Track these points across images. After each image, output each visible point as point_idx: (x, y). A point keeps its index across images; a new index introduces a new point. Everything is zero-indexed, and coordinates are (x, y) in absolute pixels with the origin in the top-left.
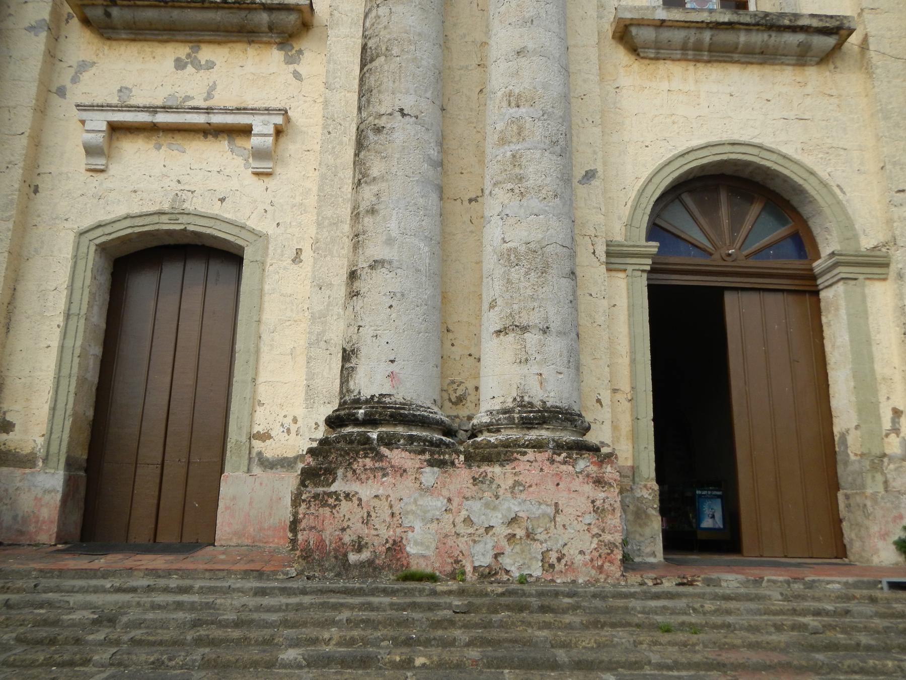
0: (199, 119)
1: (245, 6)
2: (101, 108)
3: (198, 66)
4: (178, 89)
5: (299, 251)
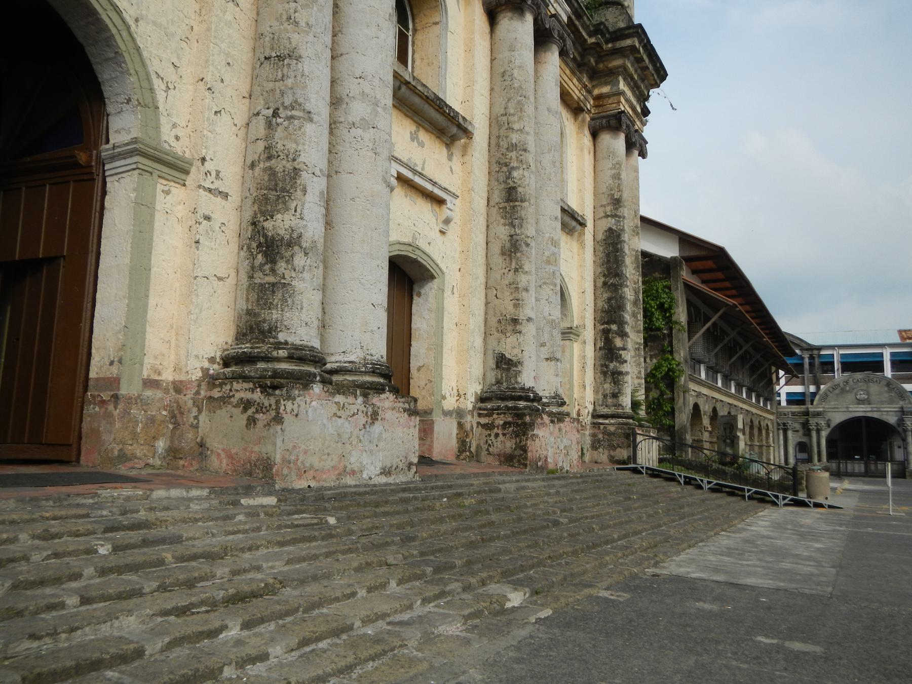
0: (429, 187)
3: (419, 143)
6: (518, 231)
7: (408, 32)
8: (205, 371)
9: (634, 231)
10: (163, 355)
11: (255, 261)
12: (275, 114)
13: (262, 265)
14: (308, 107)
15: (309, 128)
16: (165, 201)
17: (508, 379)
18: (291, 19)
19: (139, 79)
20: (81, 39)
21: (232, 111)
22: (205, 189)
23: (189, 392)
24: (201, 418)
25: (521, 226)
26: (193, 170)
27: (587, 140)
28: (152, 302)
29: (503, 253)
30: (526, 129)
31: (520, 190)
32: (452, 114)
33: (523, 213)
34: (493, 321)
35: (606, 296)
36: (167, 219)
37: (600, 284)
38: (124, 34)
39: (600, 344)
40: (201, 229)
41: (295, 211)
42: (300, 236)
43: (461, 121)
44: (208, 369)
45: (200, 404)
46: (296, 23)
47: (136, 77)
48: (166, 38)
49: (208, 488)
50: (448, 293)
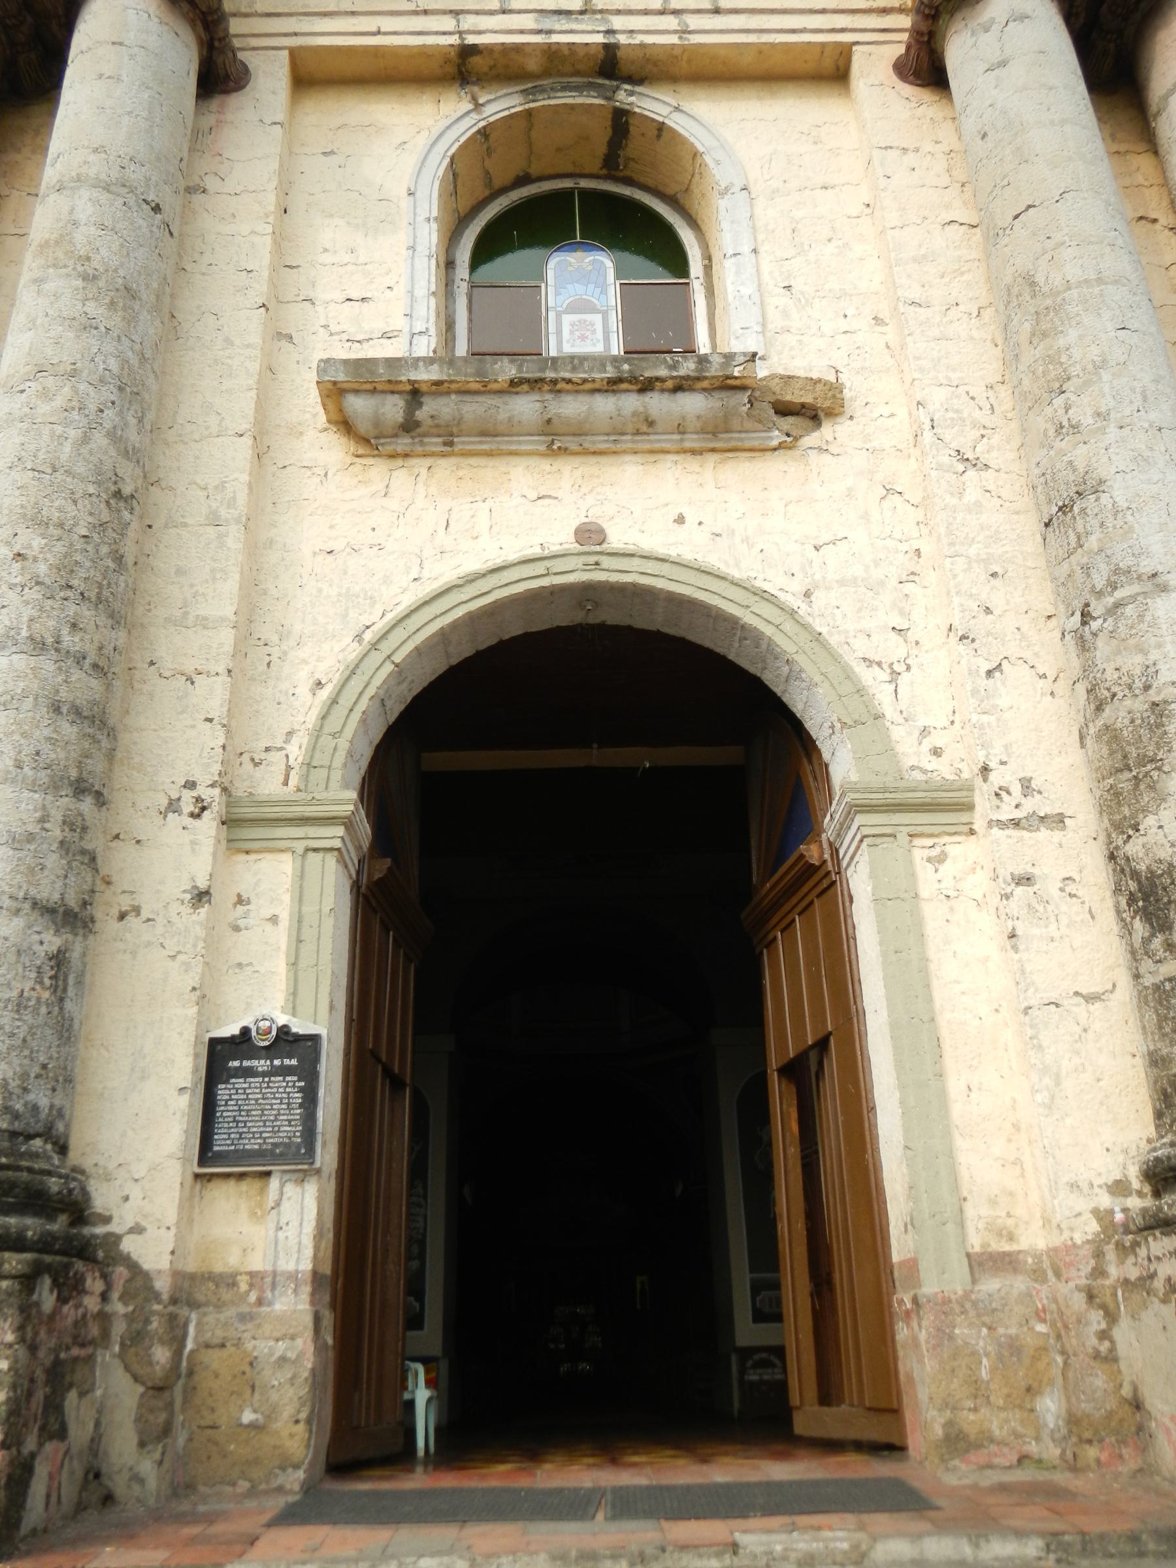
8: (1102, 1216)
10: (1011, 1194)
11: (1134, 936)
12: (1086, 617)
13: (1146, 941)
14: (1146, 566)
15: (1162, 607)
16: (939, 876)
18: (1062, 427)
19: (832, 685)
20: (752, 669)
21: (1027, 655)
22: (1001, 824)
23: (1073, 1273)
24: (1117, 1333)
26: (978, 799)
28: (955, 1085)
36: (952, 909)
38: (788, 626)
40: (1013, 906)
44: (1111, 1212)
45: (1108, 1300)
46: (1075, 427)
47: (826, 685)
48: (871, 594)
49: (1041, 1534)
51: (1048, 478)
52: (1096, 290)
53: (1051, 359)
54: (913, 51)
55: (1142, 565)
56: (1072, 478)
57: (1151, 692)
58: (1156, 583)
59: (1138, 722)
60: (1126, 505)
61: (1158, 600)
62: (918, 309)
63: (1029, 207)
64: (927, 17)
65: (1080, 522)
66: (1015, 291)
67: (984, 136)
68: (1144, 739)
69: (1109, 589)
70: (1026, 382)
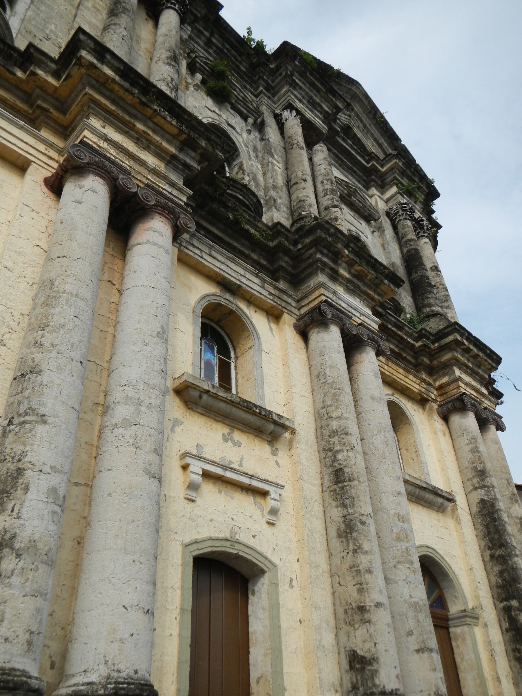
0: (246, 480)
1: (267, 418)
2: (199, 458)
3: (234, 443)
4: (226, 455)
5: (291, 579)
6: (351, 511)
7: (230, 360)
9: (511, 499)
12: (10, 423)
14: (42, 411)
15: (41, 429)
17: (364, 682)
18: (37, 343)
25: (353, 505)
27: (439, 424)
29: (339, 536)
30: (345, 415)
31: (346, 470)
32: (263, 413)
33: (353, 492)
34: (340, 611)
35: (497, 569)
37: (487, 558)
39: (506, 625)
41: (12, 511)
42: (14, 537)
43: (275, 417)
46: (42, 345)
50: (283, 587)
51: (22, 361)
52: (74, 298)
53: (46, 316)
54: (53, 178)
55: (41, 409)
56: (31, 364)
57: (20, 463)
58: (43, 419)
59: (9, 474)
60: (46, 384)
61: (40, 426)
62: (7, 271)
63: (64, 256)
64: (62, 170)
65: (26, 383)
66: (45, 284)
67: (62, 223)
68: (8, 482)
69: (24, 415)
70: (33, 320)
